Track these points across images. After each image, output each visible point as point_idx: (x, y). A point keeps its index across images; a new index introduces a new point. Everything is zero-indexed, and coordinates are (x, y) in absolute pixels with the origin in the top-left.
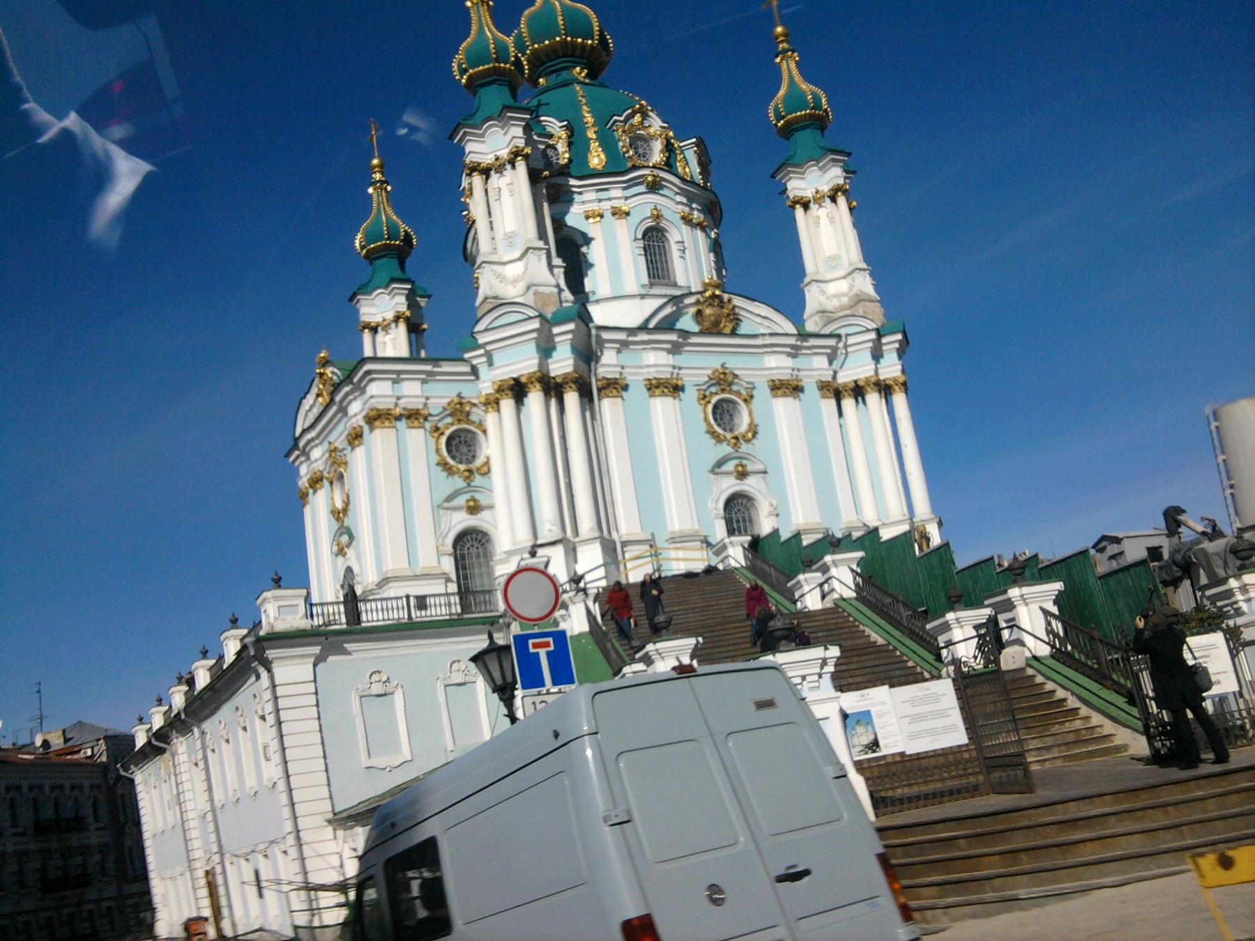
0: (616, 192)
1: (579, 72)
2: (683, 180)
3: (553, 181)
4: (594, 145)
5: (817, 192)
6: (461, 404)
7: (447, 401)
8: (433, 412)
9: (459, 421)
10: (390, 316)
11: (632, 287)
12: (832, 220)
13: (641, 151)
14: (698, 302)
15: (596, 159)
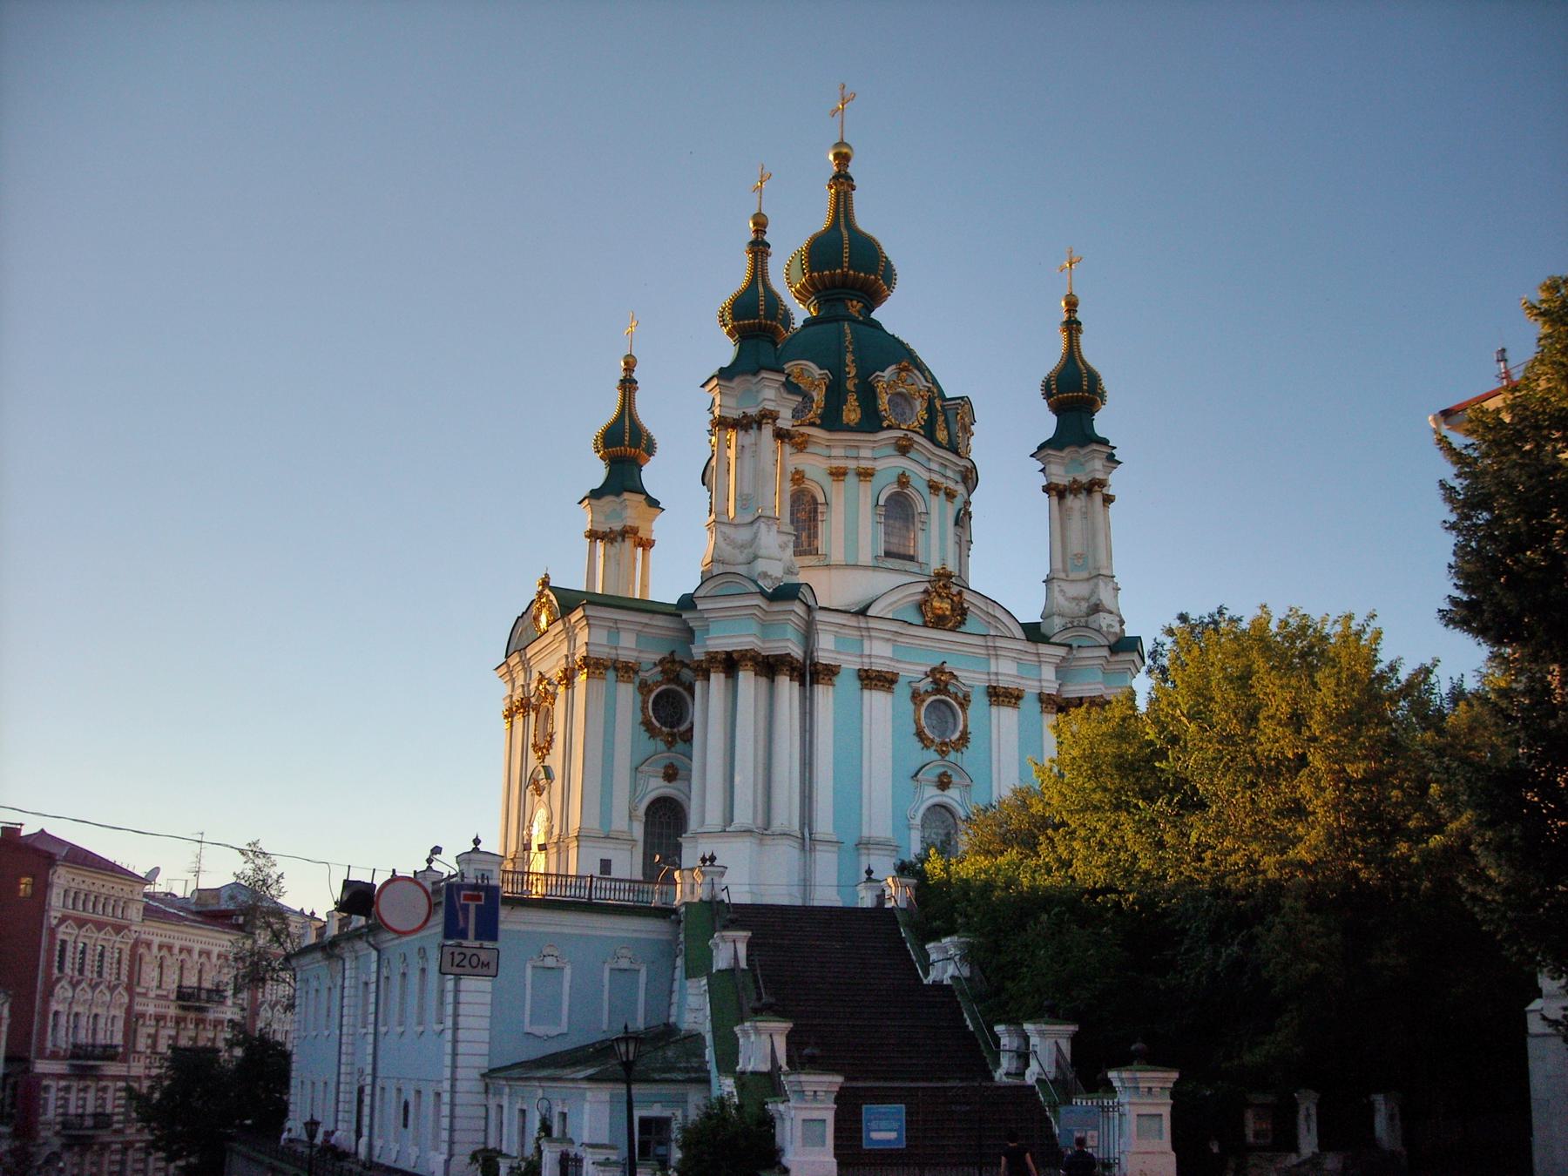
0: (864, 453)
1: (855, 307)
2: (938, 445)
3: (803, 430)
4: (852, 401)
5: (1075, 481)
6: (673, 662)
7: (657, 657)
8: (644, 666)
9: (669, 681)
10: (617, 527)
11: (865, 557)
12: (1085, 515)
13: (899, 410)
14: (926, 591)
15: (851, 414)
